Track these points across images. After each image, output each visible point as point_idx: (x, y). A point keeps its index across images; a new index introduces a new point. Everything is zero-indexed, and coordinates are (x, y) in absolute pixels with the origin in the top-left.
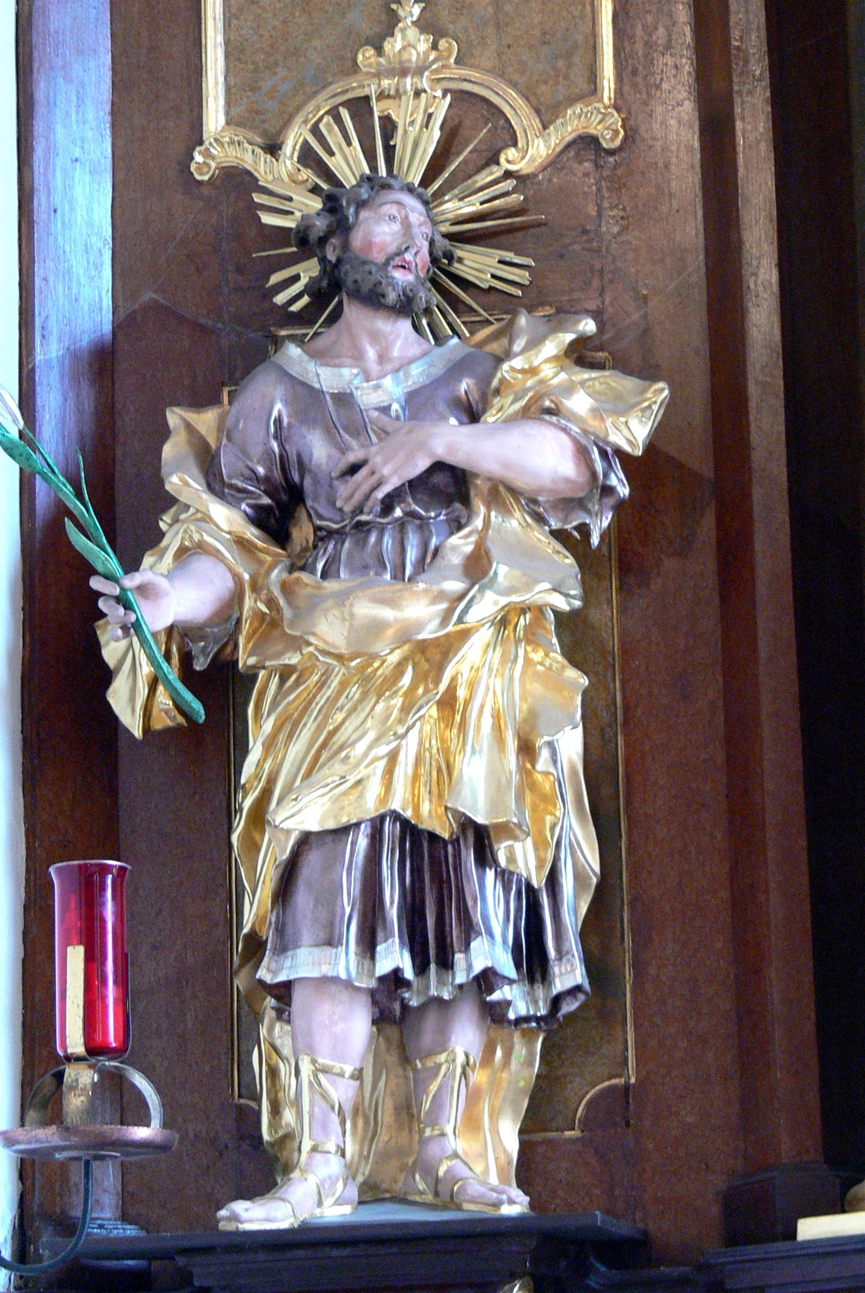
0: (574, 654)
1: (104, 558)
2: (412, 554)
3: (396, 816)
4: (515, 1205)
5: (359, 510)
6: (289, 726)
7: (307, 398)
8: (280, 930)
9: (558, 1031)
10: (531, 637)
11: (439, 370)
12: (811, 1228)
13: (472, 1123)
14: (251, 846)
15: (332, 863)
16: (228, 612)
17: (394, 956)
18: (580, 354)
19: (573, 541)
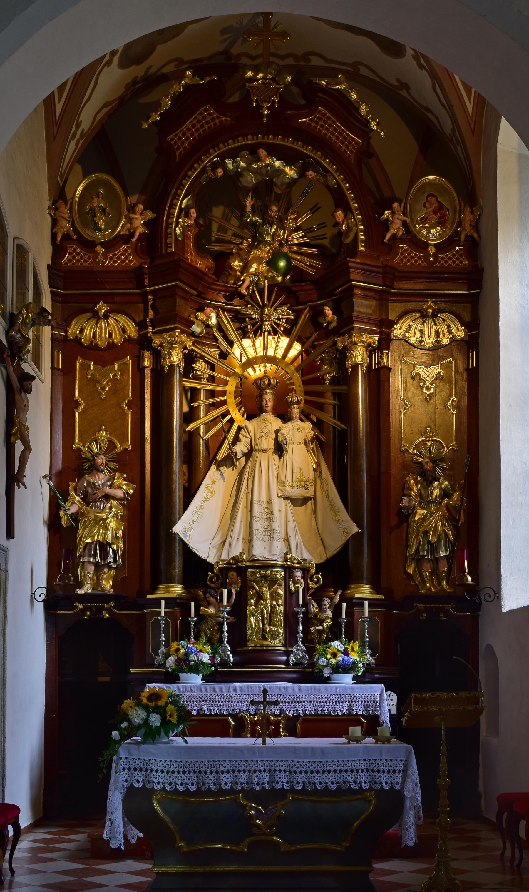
2: (102, 506)
3: (99, 541)
4: (112, 592)
5: (95, 499)
6: (85, 528)
7: (88, 483)
8: (83, 555)
11: (106, 480)
12: (149, 596)
13: (106, 580)
14: (80, 542)
16: (77, 513)
17: (98, 559)
18: (125, 479)
19: (122, 505)
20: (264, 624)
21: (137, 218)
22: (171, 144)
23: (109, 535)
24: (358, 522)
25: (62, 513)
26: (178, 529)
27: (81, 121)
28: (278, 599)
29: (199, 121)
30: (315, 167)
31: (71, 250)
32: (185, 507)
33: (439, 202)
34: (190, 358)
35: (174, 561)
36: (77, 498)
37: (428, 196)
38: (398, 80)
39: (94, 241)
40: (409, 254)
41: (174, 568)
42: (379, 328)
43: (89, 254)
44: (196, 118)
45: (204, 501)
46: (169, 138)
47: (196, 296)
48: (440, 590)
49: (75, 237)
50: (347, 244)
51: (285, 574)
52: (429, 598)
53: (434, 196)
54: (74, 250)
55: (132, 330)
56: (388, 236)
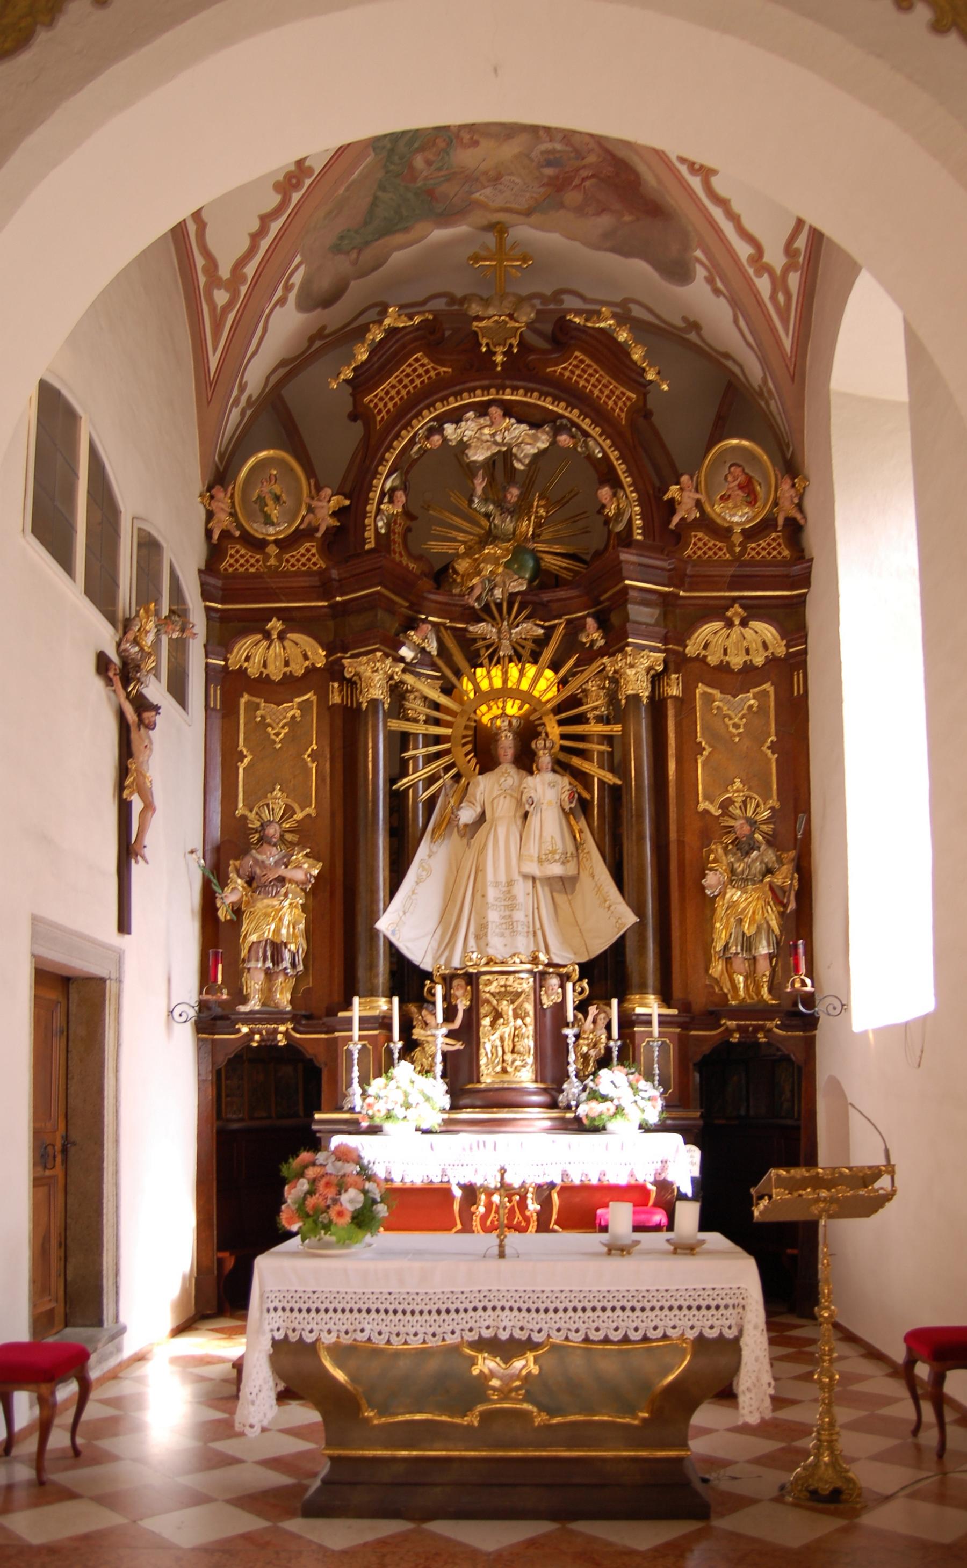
0: (303, 911)
1: (218, 890)
7: (256, 861)
9: (298, 978)
10: (296, 907)
15: (258, 947)
16: (240, 902)
17: (269, 964)
19: (304, 890)
20: (504, 1053)
21: (322, 507)
22: (369, 408)
23: (284, 931)
24: (639, 910)
25: (218, 904)
26: (384, 924)
27: (246, 382)
28: (525, 1017)
29: (408, 375)
30: (570, 430)
31: (233, 552)
32: (392, 893)
33: (746, 474)
34: (398, 692)
35: (377, 966)
36: (239, 881)
37: (731, 466)
38: (685, 319)
39: (264, 539)
40: (705, 544)
41: (377, 975)
42: (665, 644)
43: (258, 556)
44: (403, 371)
45: (417, 883)
46: (366, 399)
47: (406, 608)
48: (759, 1001)
49: (237, 533)
50: (618, 533)
51: (535, 981)
52: (741, 1012)
53: (739, 466)
54: (237, 552)
55: (319, 657)
56: (676, 520)
